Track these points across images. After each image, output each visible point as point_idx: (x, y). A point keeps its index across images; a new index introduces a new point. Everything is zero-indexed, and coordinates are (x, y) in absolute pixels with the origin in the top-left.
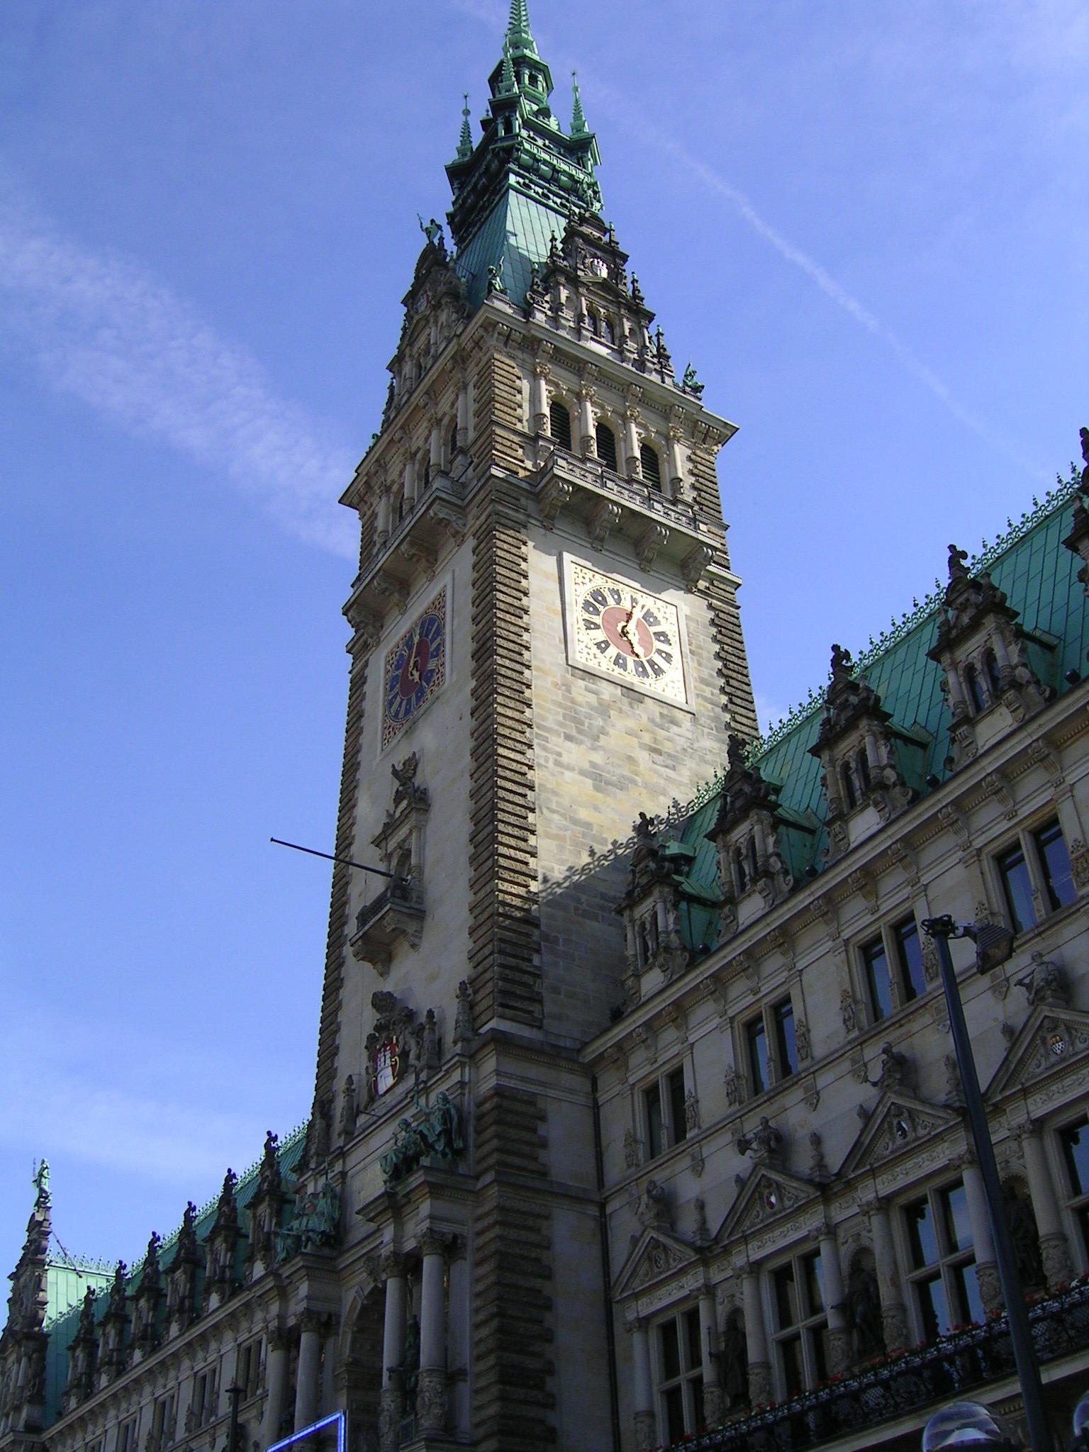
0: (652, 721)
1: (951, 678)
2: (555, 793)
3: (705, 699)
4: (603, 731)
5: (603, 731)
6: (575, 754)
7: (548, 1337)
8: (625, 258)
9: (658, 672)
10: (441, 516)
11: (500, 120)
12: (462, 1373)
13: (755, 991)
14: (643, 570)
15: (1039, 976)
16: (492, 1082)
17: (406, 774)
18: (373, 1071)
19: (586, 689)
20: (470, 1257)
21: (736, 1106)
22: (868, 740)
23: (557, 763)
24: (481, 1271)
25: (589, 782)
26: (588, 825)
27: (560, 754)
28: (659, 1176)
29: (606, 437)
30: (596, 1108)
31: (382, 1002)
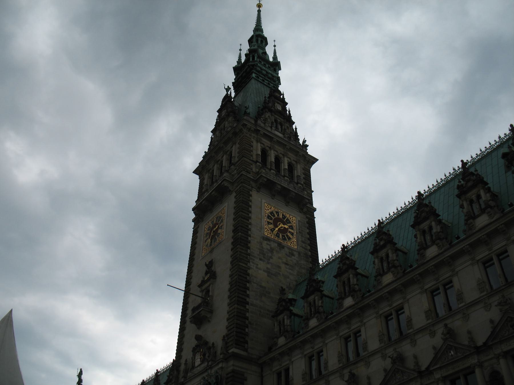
0: (286, 254)
1: (376, 261)
3: (303, 247)
4: (271, 258)
5: (271, 258)
6: (262, 265)
8: (287, 104)
10: (226, 185)
11: (251, 56)
13: (313, 348)
14: (287, 206)
15: (395, 355)
16: (232, 368)
17: (210, 265)
18: (194, 359)
19: (267, 244)
22: (351, 276)
25: (266, 274)
27: (257, 265)
29: (278, 161)
30: (262, 377)
31: (198, 338)
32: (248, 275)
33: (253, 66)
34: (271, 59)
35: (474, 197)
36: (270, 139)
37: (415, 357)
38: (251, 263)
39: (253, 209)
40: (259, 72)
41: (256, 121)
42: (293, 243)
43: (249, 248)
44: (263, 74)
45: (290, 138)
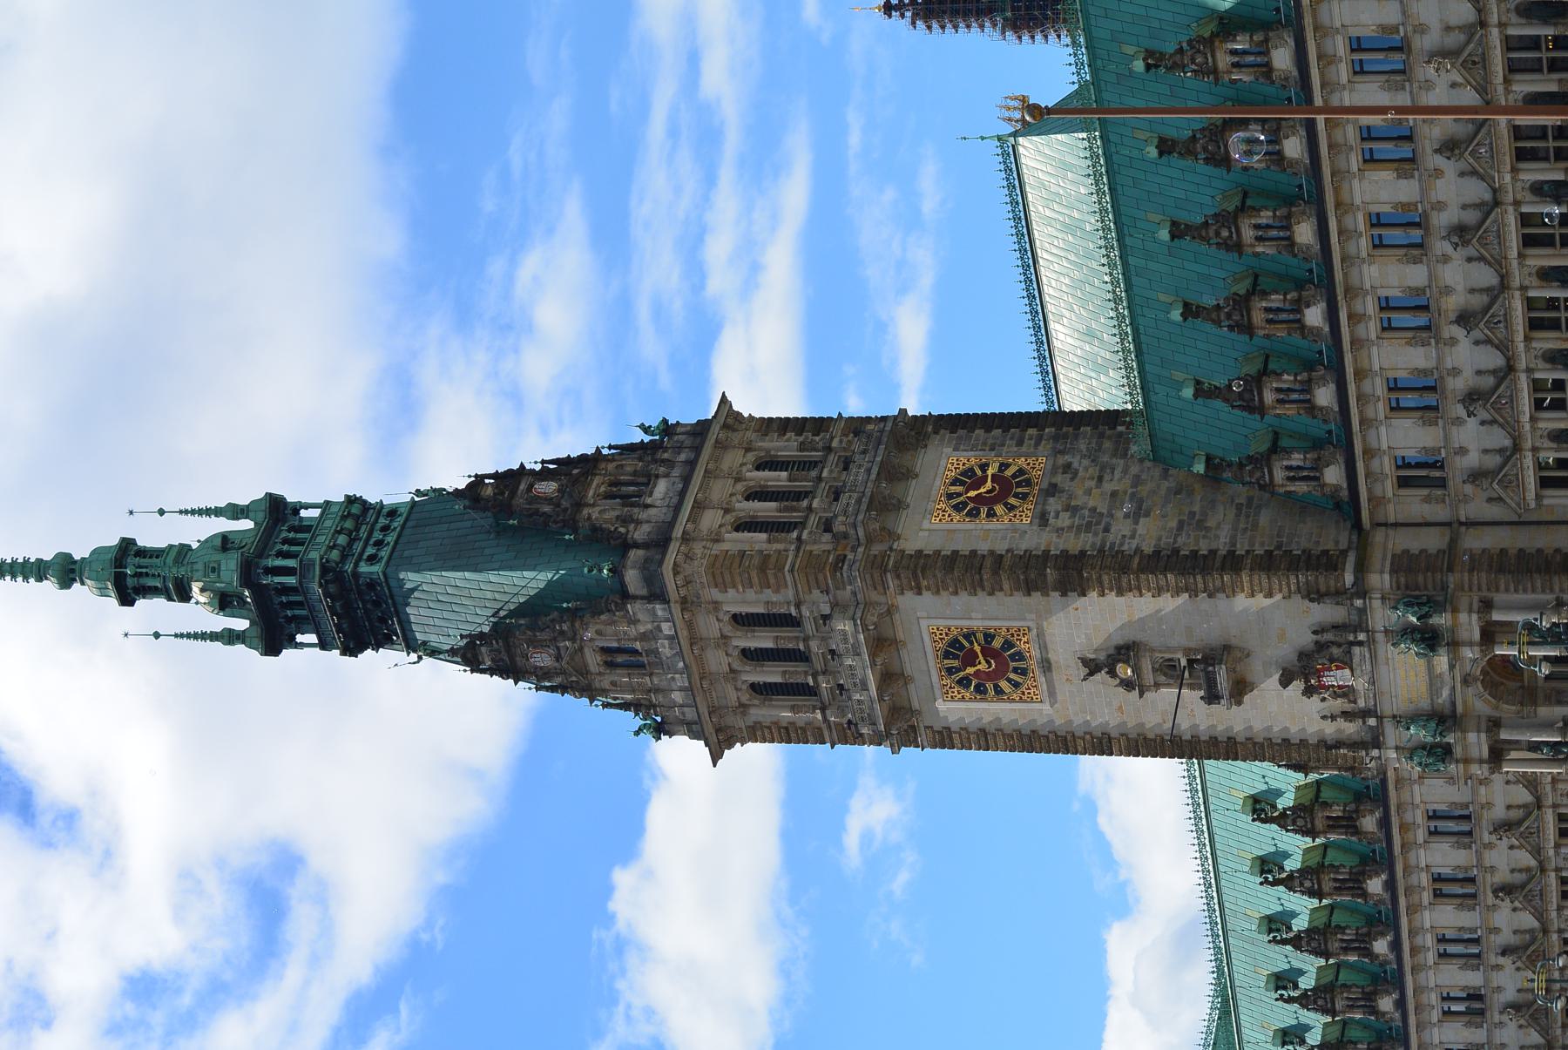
2: (1160, 539)
3: (1037, 444)
4: (1093, 510)
6: (1120, 528)
7: (1539, 551)
9: (1021, 472)
12: (1557, 599)
15: (1455, 239)
16: (1387, 577)
19: (1057, 517)
20: (1490, 595)
21: (1440, 422)
23: (1132, 537)
24: (1502, 587)
26: (1181, 523)
28: (1459, 480)
30: (1396, 525)
32: (1157, 553)
33: (325, 570)
34: (246, 524)
35: (1230, 59)
36: (699, 506)
37: (1464, 207)
38: (1126, 547)
39: (964, 547)
40: (345, 554)
41: (636, 545)
42: (1036, 463)
43: (1083, 553)
44: (352, 541)
45: (670, 464)
